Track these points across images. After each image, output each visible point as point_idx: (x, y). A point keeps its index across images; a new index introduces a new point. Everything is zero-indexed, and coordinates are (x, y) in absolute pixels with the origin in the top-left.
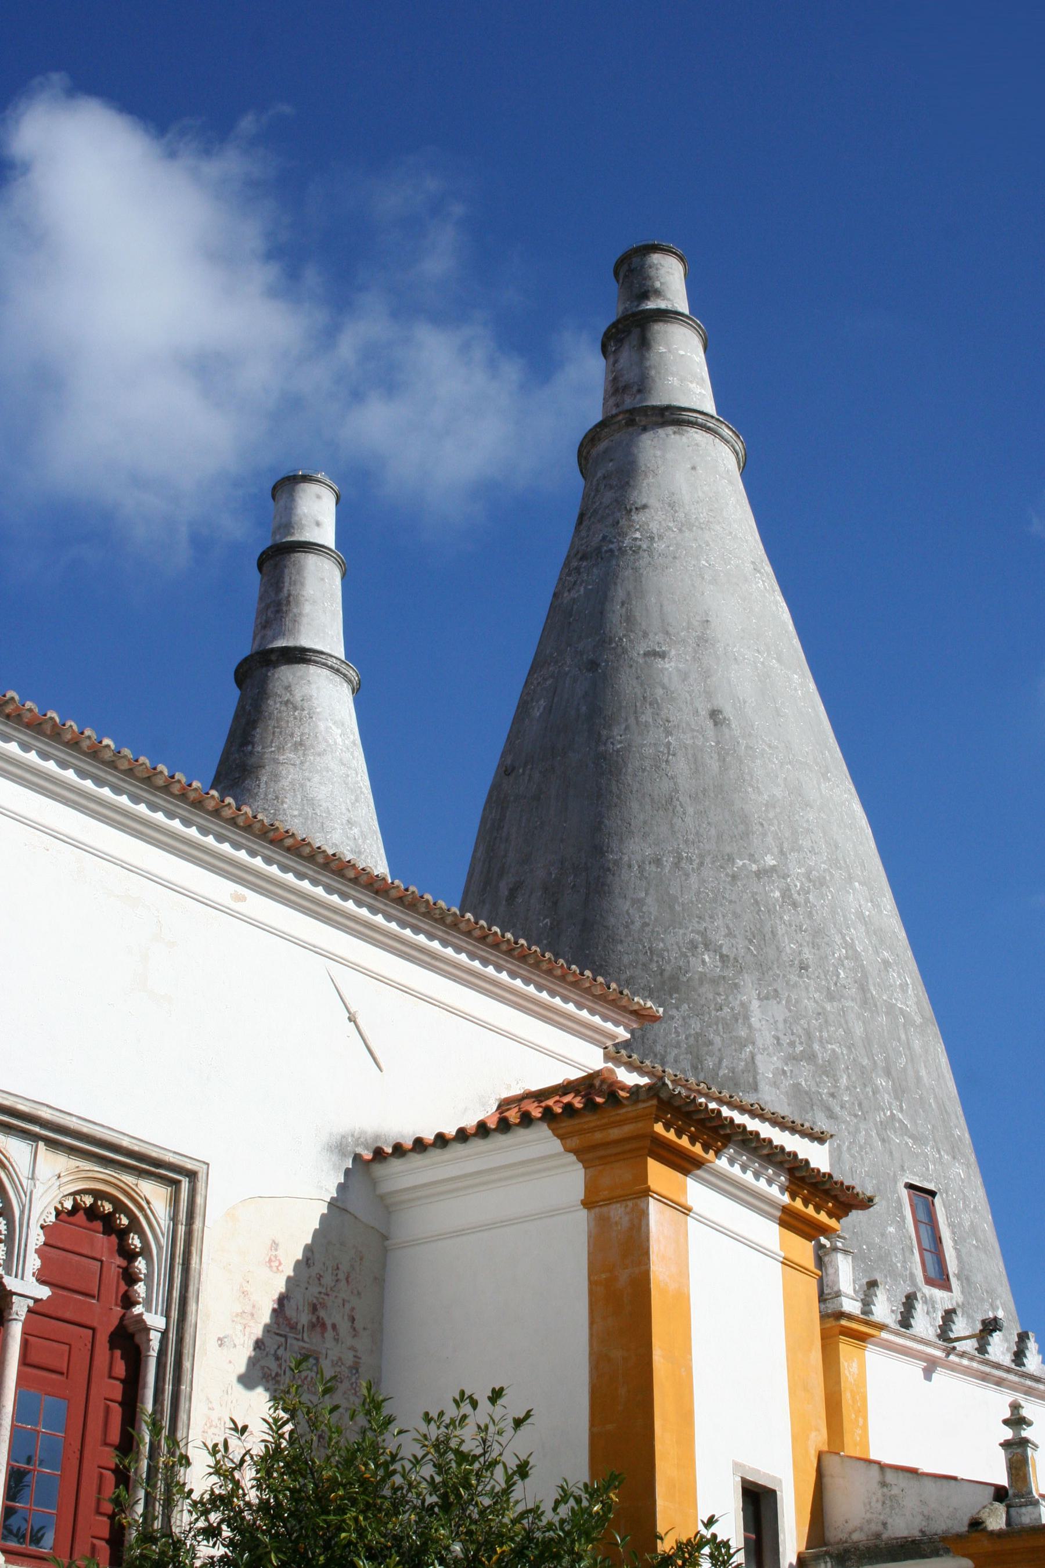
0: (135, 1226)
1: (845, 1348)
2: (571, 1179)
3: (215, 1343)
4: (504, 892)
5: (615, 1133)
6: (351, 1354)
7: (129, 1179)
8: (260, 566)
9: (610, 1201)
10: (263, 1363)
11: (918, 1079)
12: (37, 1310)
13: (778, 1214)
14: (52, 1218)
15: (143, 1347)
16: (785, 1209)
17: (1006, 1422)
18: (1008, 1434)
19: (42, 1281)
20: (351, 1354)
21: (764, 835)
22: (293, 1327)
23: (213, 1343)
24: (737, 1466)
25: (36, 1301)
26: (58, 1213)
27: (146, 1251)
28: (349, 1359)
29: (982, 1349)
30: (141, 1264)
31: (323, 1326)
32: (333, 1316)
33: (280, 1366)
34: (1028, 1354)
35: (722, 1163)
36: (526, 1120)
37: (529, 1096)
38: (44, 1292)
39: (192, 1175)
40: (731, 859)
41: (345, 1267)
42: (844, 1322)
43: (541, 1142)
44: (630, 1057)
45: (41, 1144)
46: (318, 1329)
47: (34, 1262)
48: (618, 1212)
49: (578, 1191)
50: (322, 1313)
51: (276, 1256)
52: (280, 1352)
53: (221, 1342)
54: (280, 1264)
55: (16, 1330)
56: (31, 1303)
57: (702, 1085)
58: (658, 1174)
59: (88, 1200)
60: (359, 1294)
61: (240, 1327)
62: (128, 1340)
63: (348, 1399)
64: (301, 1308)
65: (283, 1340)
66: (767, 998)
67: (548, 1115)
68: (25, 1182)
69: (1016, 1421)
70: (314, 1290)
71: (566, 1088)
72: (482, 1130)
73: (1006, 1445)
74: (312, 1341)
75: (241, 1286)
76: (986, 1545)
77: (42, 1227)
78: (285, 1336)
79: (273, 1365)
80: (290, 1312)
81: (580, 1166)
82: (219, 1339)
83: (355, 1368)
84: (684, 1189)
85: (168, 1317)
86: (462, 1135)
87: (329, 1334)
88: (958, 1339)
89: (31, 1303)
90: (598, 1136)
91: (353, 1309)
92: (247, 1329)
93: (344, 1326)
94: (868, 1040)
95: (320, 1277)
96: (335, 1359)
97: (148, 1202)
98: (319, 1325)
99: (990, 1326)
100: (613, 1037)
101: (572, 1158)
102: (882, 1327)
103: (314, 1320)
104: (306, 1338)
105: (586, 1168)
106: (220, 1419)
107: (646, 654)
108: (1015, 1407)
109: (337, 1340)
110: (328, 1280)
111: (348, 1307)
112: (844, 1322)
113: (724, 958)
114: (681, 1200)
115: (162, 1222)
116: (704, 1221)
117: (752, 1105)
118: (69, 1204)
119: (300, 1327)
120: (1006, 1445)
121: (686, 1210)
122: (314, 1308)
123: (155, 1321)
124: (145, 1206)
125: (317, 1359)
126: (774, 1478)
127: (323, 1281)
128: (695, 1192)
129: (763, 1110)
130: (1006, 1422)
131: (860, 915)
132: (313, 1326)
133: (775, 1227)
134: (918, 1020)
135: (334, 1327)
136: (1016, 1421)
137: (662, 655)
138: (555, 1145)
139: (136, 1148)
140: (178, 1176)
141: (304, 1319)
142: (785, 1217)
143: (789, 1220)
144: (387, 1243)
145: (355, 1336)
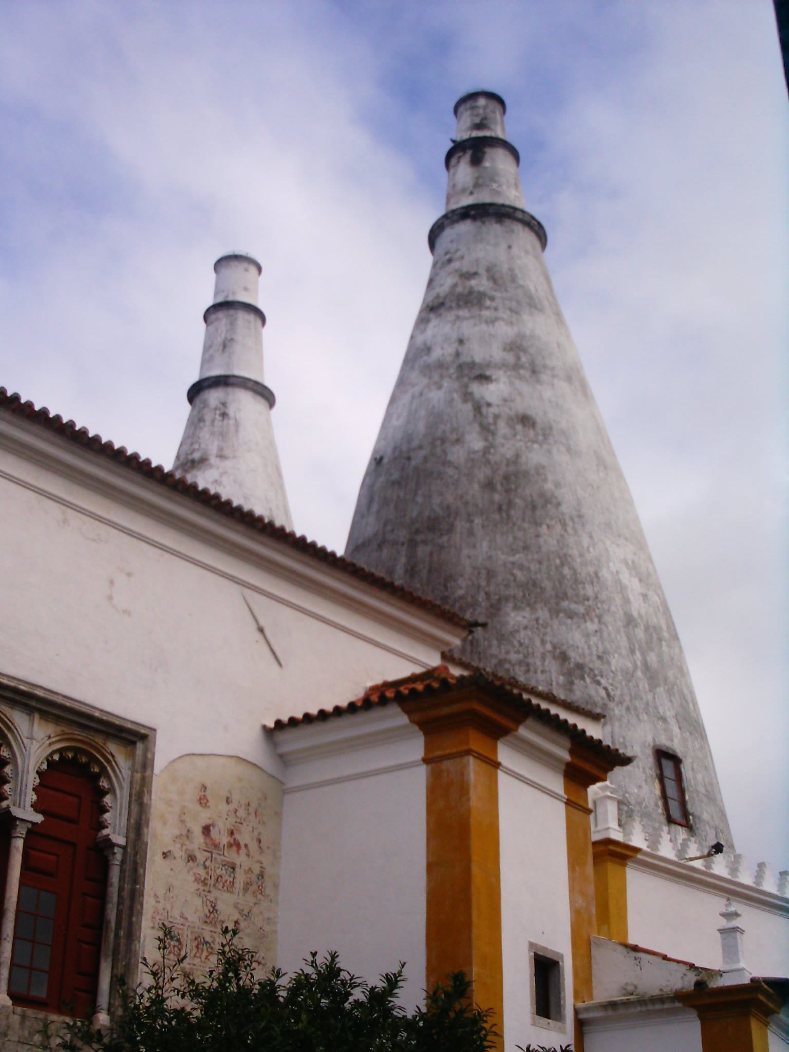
0: (103, 772)
1: (611, 868)
3: (160, 855)
5: (446, 711)
6: (258, 865)
7: (99, 740)
8: (206, 318)
10: (196, 870)
12: (34, 831)
14: (45, 766)
15: (111, 857)
16: (568, 765)
18: (724, 923)
19: (36, 811)
20: (258, 865)
22: (216, 846)
23: (159, 856)
24: (532, 945)
25: (34, 824)
26: (51, 763)
27: (112, 790)
28: (257, 869)
29: (708, 866)
30: (108, 799)
31: (238, 846)
32: (244, 837)
33: (207, 873)
34: (741, 869)
35: (522, 731)
36: (383, 701)
38: (39, 818)
39: (144, 737)
41: (254, 805)
42: (611, 847)
45: (37, 716)
46: (235, 848)
47: (32, 797)
50: (237, 836)
51: (204, 796)
52: (207, 863)
53: (165, 855)
54: (208, 801)
56: (30, 826)
58: (476, 741)
60: (264, 823)
61: (178, 846)
63: (256, 897)
64: (222, 832)
65: (209, 855)
67: (400, 699)
68: (25, 741)
70: (232, 820)
71: (413, 678)
72: (352, 708)
73: (722, 931)
75: (180, 816)
77: (37, 772)
78: (211, 852)
79: (203, 873)
80: (214, 833)
81: (421, 733)
82: (164, 853)
83: (261, 875)
84: (495, 750)
85: (127, 837)
87: (243, 851)
88: (691, 859)
89: (30, 826)
91: (260, 834)
92: (184, 847)
93: (253, 846)
95: (236, 811)
96: (247, 868)
97: (113, 756)
100: (447, 644)
101: (416, 728)
102: (637, 850)
103: (232, 841)
104: (226, 854)
105: (426, 735)
106: (164, 909)
109: (248, 855)
110: (242, 813)
111: (256, 833)
112: (611, 847)
114: (493, 758)
115: (123, 771)
118: (56, 757)
119: (221, 846)
120: (722, 931)
121: (497, 765)
122: (232, 833)
123: (120, 840)
124: (111, 758)
125: (234, 869)
126: (558, 953)
127: (238, 814)
128: (505, 754)
132: (230, 845)
135: (246, 846)
138: (404, 720)
139: (105, 718)
140: (135, 737)
141: (225, 840)
145: (261, 853)
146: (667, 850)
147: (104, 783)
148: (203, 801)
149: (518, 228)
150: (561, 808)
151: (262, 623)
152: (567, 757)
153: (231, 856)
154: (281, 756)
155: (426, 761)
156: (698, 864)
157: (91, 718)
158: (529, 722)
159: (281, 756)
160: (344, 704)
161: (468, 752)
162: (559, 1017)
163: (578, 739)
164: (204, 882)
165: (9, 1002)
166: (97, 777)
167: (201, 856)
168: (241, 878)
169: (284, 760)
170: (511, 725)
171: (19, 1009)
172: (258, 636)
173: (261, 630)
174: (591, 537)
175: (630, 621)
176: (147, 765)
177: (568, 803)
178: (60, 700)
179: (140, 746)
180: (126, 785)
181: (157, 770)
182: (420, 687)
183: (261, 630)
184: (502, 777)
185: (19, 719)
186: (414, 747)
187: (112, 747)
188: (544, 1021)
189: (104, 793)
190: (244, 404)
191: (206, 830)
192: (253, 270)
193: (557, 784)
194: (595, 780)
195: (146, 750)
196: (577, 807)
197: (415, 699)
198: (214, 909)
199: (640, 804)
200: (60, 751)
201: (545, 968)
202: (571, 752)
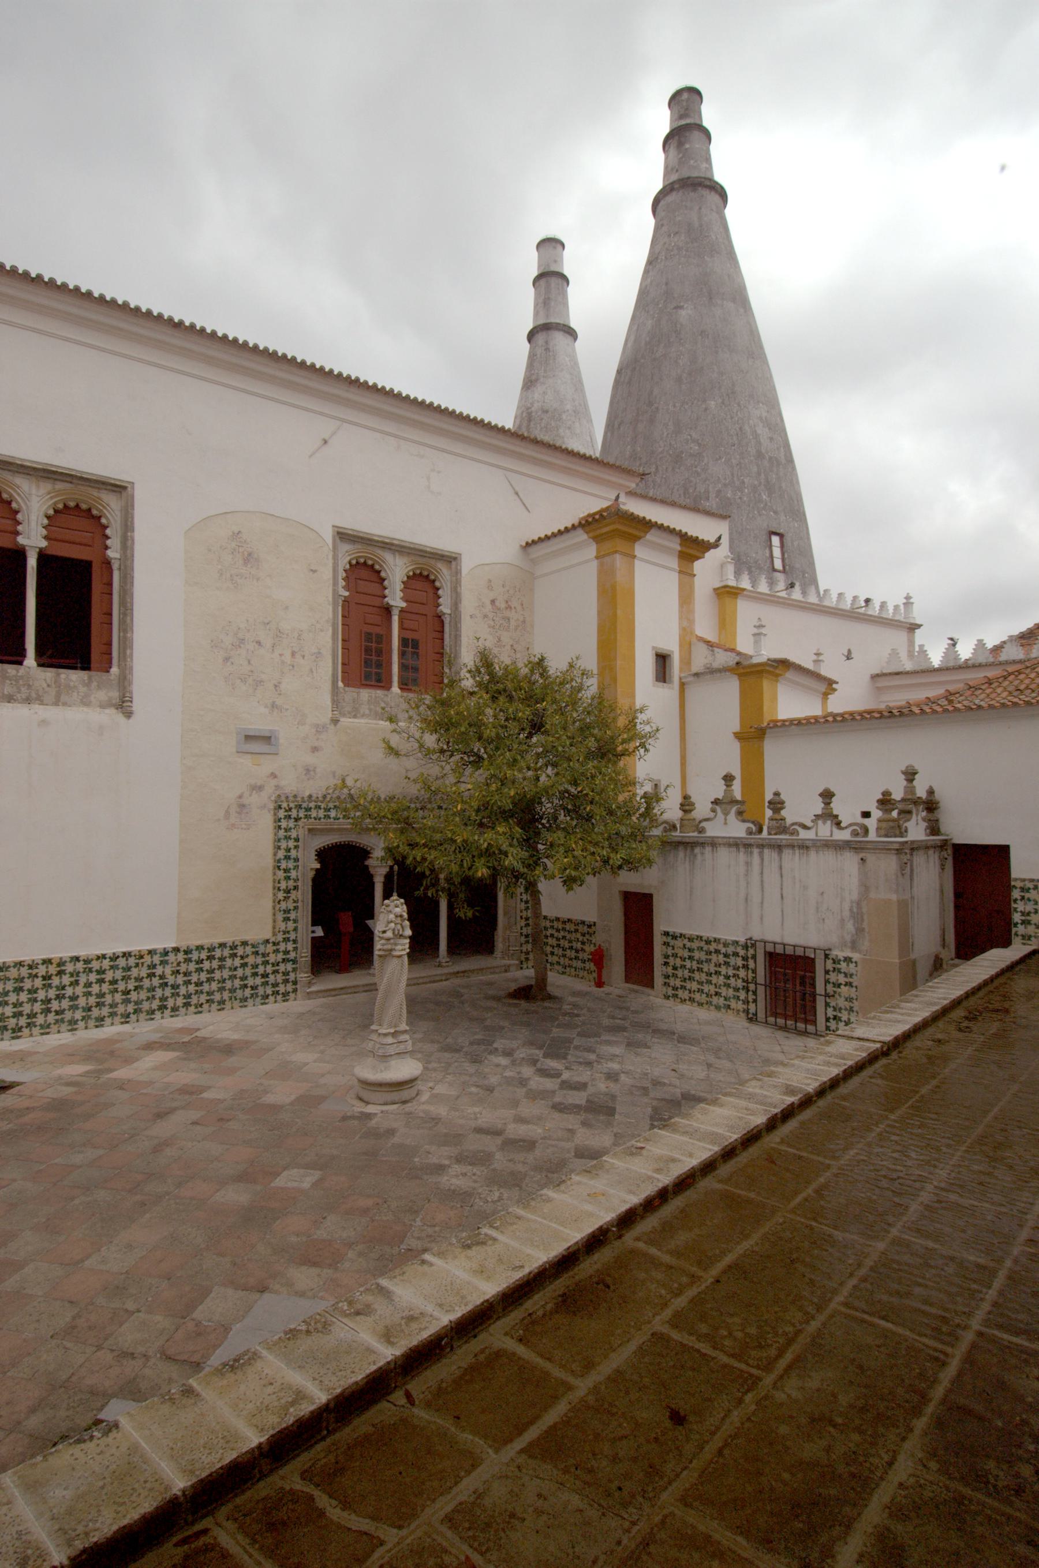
4: (616, 426)
7: (432, 562)
9: (604, 556)
11: (780, 487)
12: (402, 611)
14: (405, 579)
21: (720, 388)
22: (499, 609)
24: (654, 648)
28: (521, 619)
30: (440, 592)
32: (514, 603)
35: (649, 537)
37: (589, 515)
38: (404, 605)
39: (455, 559)
40: (704, 401)
43: (581, 536)
48: (607, 559)
53: (471, 616)
55: (395, 619)
58: (620, 544)
59: (418, 572)
62: (439, 618)
66: (717, 460)
71: (600, 513)
74: (507, 613)
76: (742, 671)
79: (492, 623)
80: (497, 603)
83: (524, 622)
86: (554, 535)
87: (513, 610)
90: (598, 532)
93: (519, 608)
94: (759, 474)
98: (509, 608)
99: (792, 585)
102: (744, 590)
107: (675, 308)
110: (512, 592)
113: (699, 445)
116: (642, 560)
118: (411, 573)
120: (754, 635)
128: (640, 550)
131: (761, 418)
134: (784, 461)
137: (681, 308)
138: (585, 537)
140: (450, 559)
141: (503, 605)
146: (763, 587)
147: (437, 584)
148: (490, 588)
149: (705, 192)
150: (675, 577)
151: (517, 489)
152: (679, 548)
153: (507, 613)
154: (532, 560)
155: (597, 558)
156: (783, 594)
157: (426, 552)
158: (653, 531)
159: (532, 560)
160: (569, 525)
161: (616, 552)
162: (671, 682)
163: (685, 538)
164: (493, 627)
165: (399, 691)
166: (434, 581)
167: (491, 615)
168: (513, 623)
169: (534, 562)
170: (642, 534)
171: (405, 694)
172: (516, 497)
173: (517, 494)
174: (739, 405)
175: (760, 455)
176: (458, 572)
177: (680, 572)
178: (408, 545)
179: (454, 563)
180: (449, 584)
181: (463, 574)
182: (597, 517)
183: (517, 494)
184: (636, 562)
185: (388, 557)
186: (592, 550)
187: (440, 565)
188: (661, 684)
189: (438, 589)
190: (559, 339)
191: (493, 602)
192: (560, 247)
193: (674, 563)
194: (698, 558)
195: (457, 565)
196: (686, 574)
197: (589, 524)
198: (499, 640)
199: (756, 562)
200: (413, 570)
201: (662, 659)
202: (681, 545)
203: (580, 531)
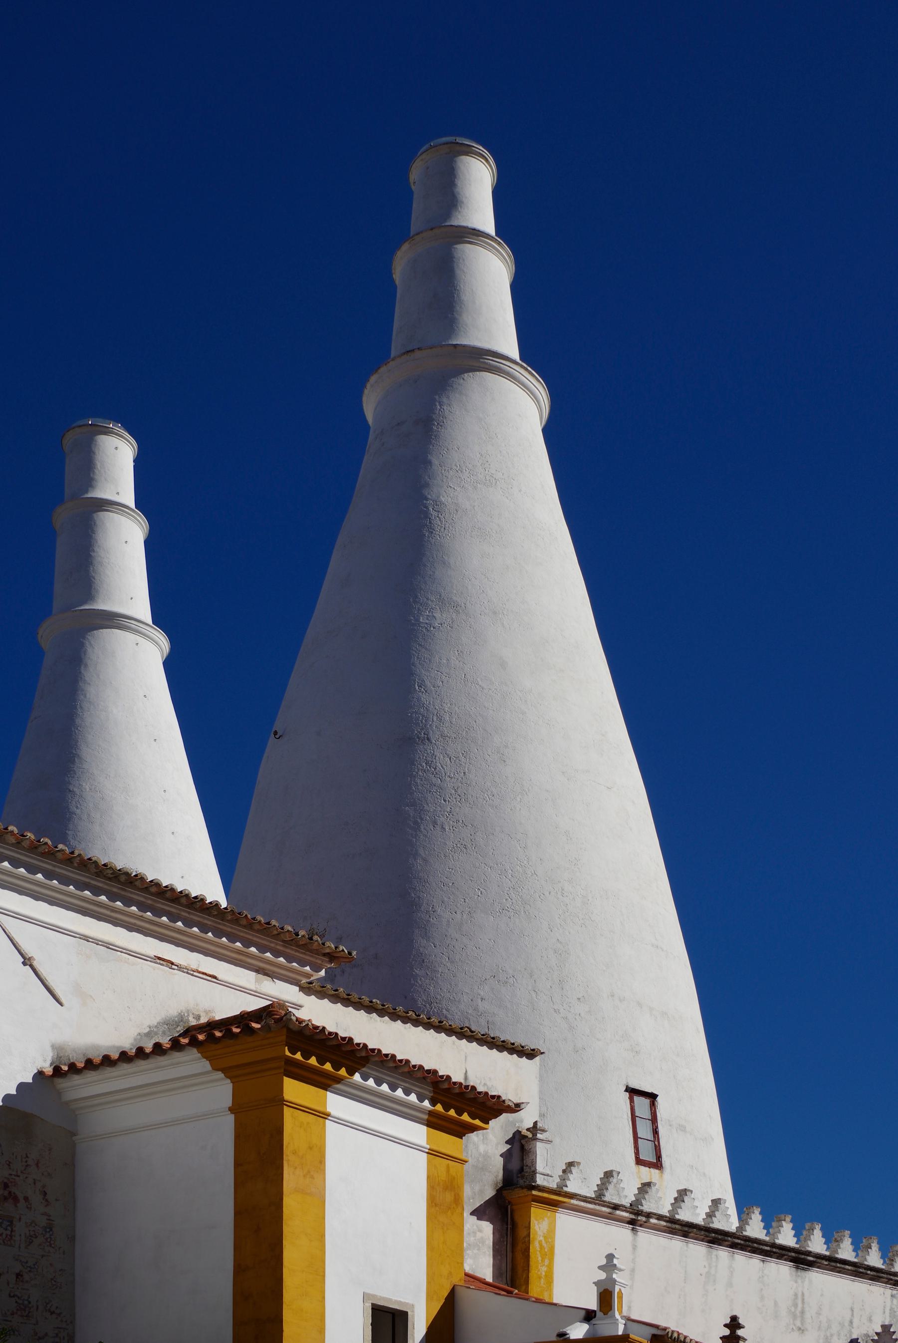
2: (222, 1091)
13: (426, 1117)
17: (600, 1268)
44: (336, 990)
49: (229, 1102)
57: (411, 1013)
69: (609, 1265)
108: (610, 1257)
117: (461, 1028)
129: (472, 1032)
130: (600, 1268)
133: (424, 1128)
136: (609, 1265)
142: (434, 1120)
143: (434, 1122)
144: (74, 1138)
203: (194, 1053)
